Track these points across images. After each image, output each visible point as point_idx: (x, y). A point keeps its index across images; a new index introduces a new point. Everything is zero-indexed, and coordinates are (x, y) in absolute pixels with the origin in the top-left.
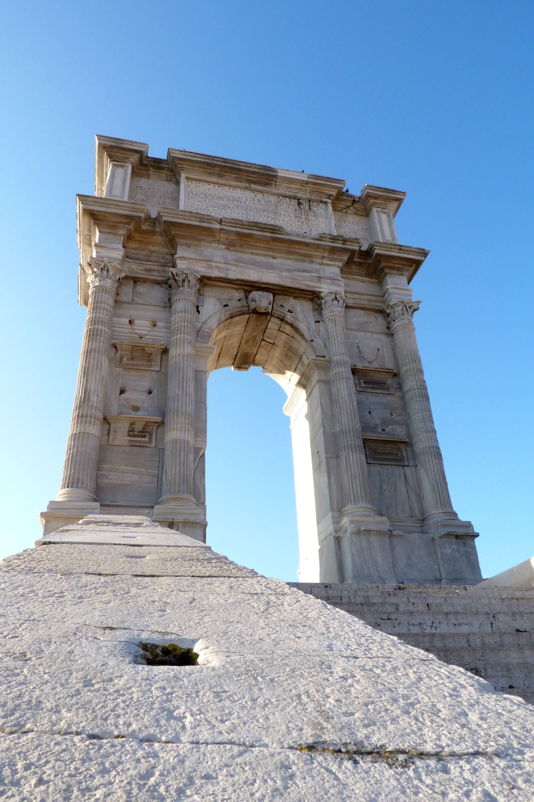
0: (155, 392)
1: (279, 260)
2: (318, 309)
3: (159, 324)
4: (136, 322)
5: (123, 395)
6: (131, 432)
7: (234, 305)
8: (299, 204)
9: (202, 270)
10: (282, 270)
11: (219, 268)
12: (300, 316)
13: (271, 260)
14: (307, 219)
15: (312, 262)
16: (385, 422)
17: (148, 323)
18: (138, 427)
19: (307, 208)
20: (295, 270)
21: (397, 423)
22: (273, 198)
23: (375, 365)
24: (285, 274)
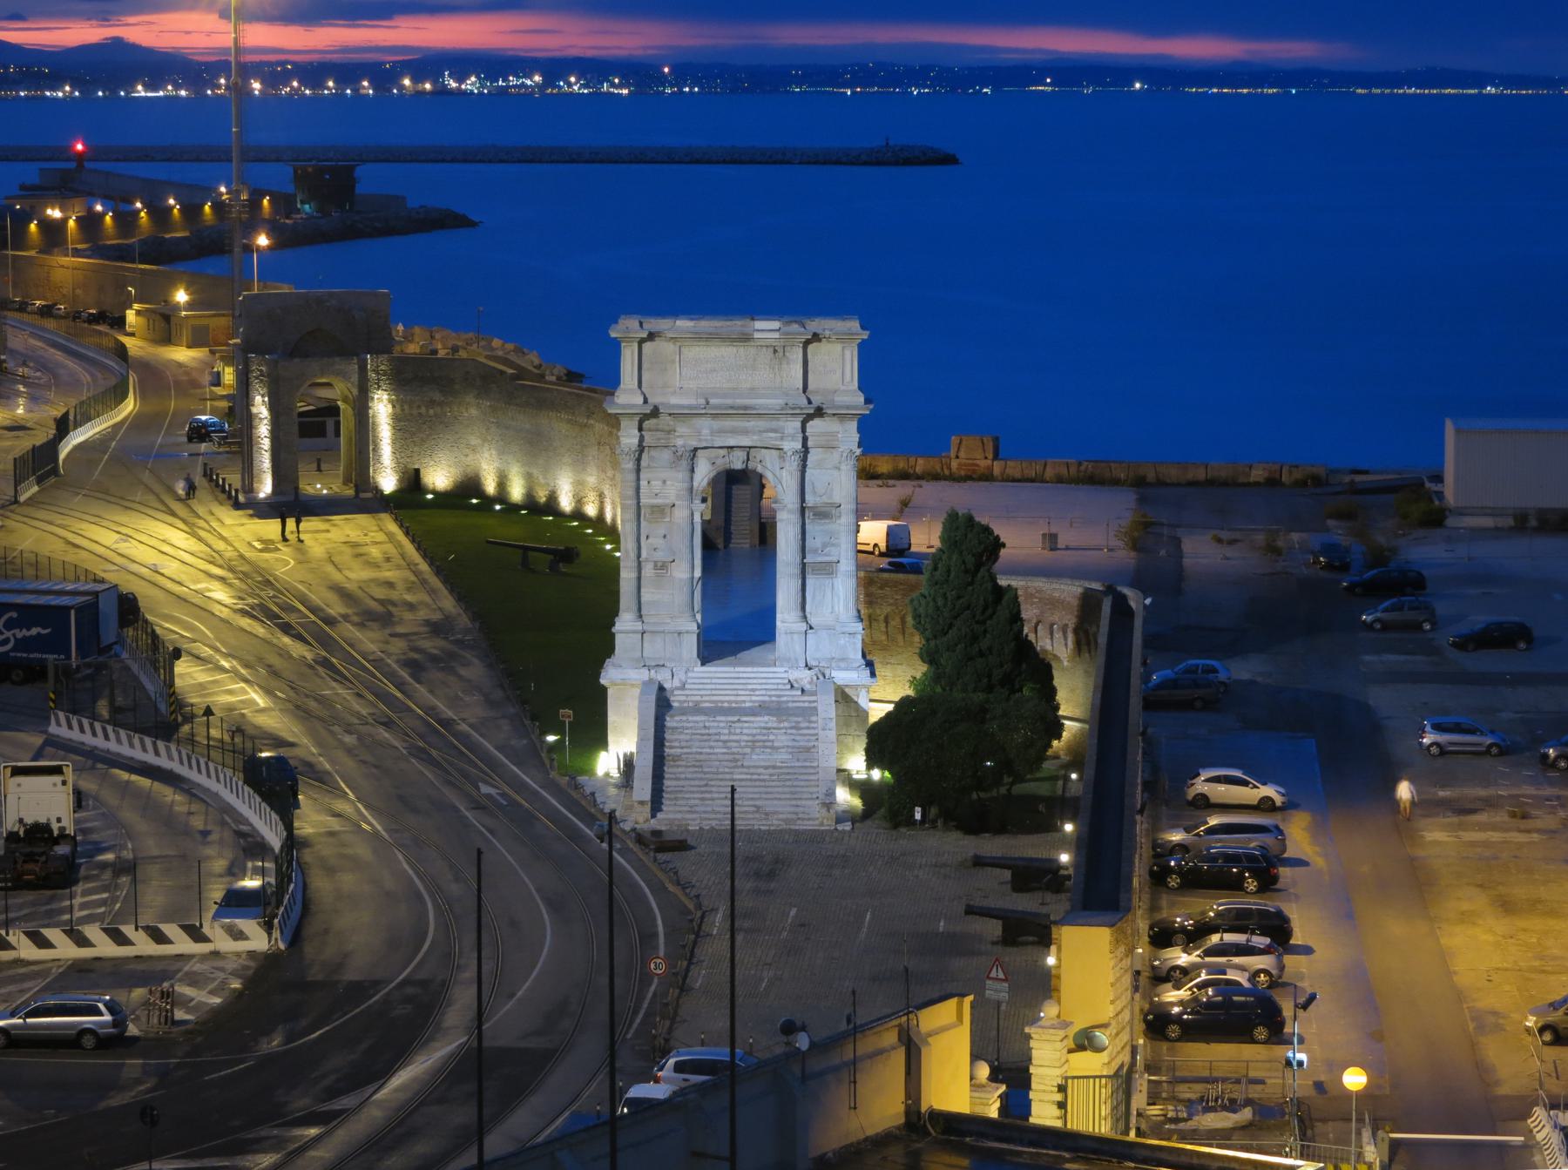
0: (668, 536)
1: (752, 423)
2: (782, 458)
3: (668, 483)
4: (653, 483)
5: (650, 540)
6: (656, 567)
7: (719, 462)
8: (775, 351)
9: (695, 444)
10: (754, 433)
11: (706, 440)
12: (769, 465)
13: (747, 424)
14: (780, 369)
15: (778, 419)
16: (825, 545)
17: (660, 483)
18: (659, 564)
19: (781, 354)
20: (764, 432)
21: (833, 545)
22: (752, 351)
23: (825, 499)
24: (755, 437)
